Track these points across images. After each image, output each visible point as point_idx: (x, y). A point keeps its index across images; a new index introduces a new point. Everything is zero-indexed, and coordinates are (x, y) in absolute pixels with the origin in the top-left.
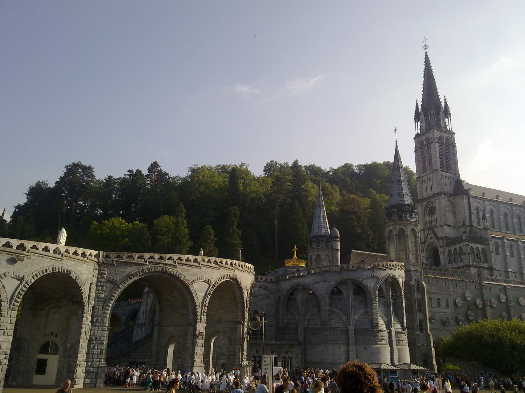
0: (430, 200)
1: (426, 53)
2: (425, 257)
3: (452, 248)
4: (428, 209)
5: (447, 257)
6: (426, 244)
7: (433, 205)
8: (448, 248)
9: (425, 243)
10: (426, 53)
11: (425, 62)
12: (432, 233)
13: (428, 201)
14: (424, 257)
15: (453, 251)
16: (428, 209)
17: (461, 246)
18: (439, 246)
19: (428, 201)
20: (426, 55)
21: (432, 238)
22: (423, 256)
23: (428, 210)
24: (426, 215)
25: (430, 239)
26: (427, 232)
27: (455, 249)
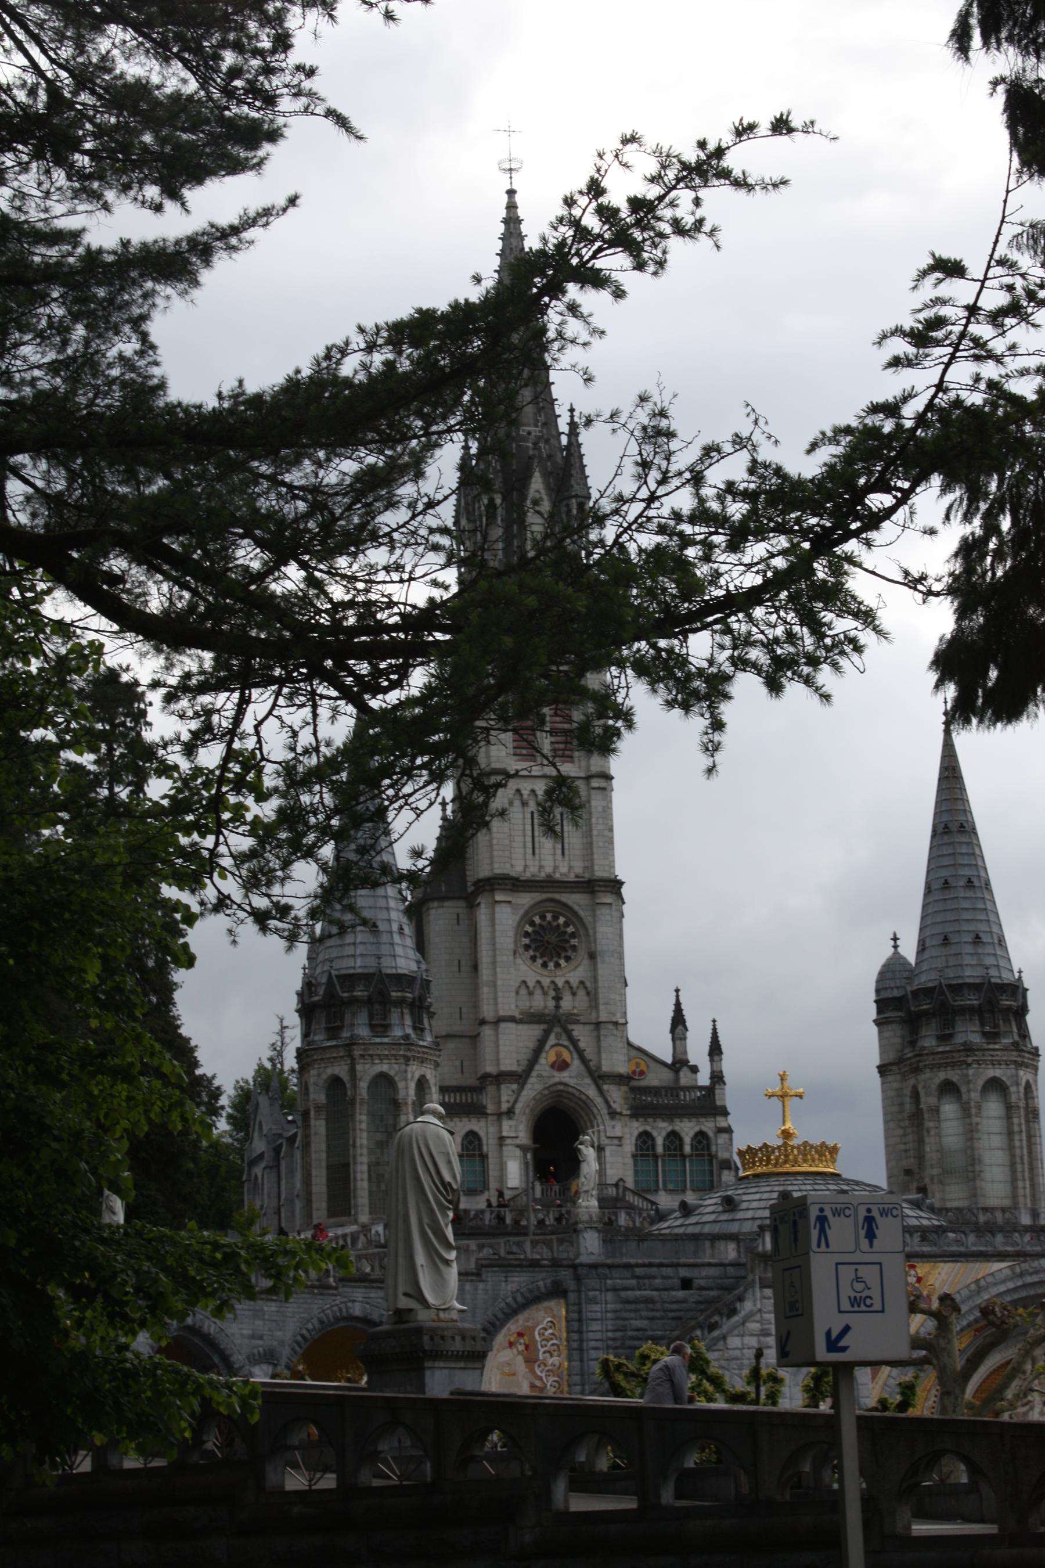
0: (557, 896)
1: (511, 193)
3: (660, 1130)
4: (529, 929)
5: (630, 1161)
6: (528, 1086)
8: (637, 1127)
9: (524, 1083)
10: (511, 193)
11: (504, 238)
12: (566, 1043)
13: (545, 896)
14: (508, 1141)
15: (660, 1141)
16: (529, 929)
17: (704, 1129)
18: (605, 1111)
19: (545, 896)
20: (511, 207)
21: (562, 1065)
22: (505, 1134)
23: (527, 934)
25: (553, 1066)
26: (530, 1033)
27: (674, 1137)
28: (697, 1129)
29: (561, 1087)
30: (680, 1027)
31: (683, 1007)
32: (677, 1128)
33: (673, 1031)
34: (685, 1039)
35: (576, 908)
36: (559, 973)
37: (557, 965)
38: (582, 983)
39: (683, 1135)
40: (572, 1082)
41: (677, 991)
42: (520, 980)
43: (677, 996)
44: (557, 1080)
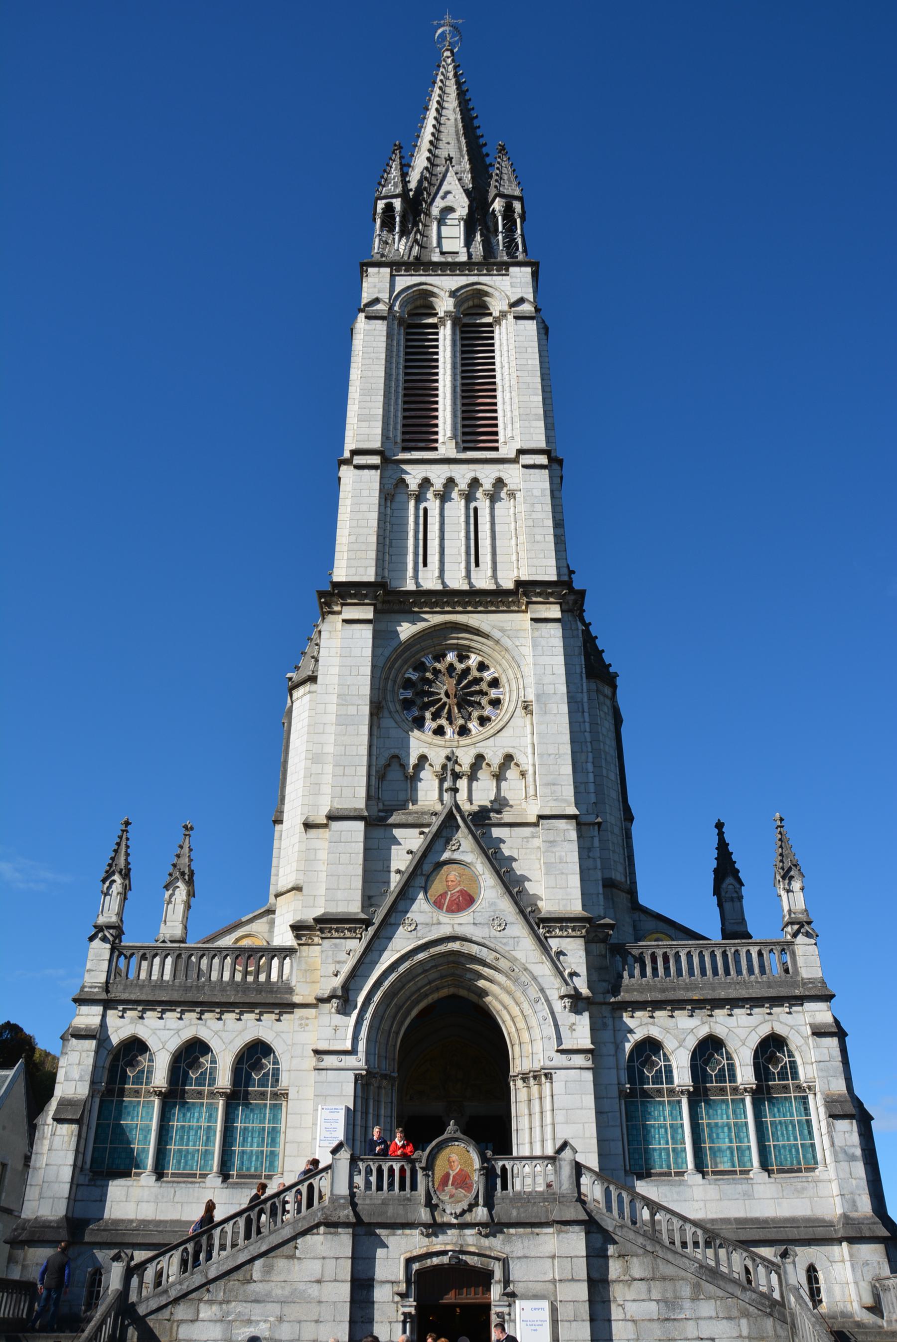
2: (349, 1061)
7: (473, 660)
14: (330, 1061)
24: (386, 714)
28: (764, 1031)
29: (455, 946)
30: (730, 880)
31: (731, 848)
32: (720, 1031)
33: (717, 891)
34: (740, 898)
35: (496, 634)
36: (464, 741)
37: (463, 731)
38: (509, 758)
39: (732, 1045)
40: (476, 933)
41: (720, 826)
42: (387, 754)
43: (721, 834)
44: (446, 931)
